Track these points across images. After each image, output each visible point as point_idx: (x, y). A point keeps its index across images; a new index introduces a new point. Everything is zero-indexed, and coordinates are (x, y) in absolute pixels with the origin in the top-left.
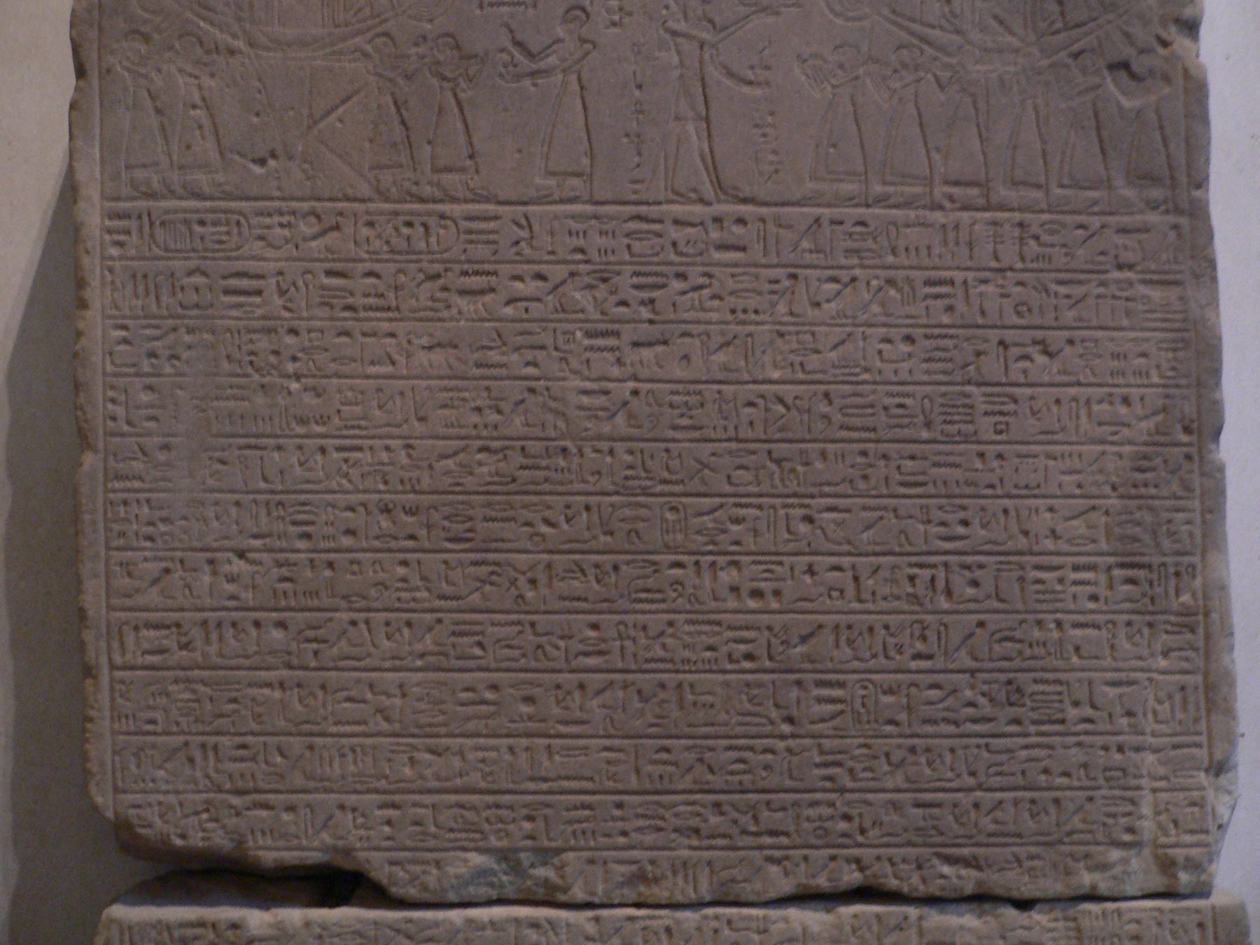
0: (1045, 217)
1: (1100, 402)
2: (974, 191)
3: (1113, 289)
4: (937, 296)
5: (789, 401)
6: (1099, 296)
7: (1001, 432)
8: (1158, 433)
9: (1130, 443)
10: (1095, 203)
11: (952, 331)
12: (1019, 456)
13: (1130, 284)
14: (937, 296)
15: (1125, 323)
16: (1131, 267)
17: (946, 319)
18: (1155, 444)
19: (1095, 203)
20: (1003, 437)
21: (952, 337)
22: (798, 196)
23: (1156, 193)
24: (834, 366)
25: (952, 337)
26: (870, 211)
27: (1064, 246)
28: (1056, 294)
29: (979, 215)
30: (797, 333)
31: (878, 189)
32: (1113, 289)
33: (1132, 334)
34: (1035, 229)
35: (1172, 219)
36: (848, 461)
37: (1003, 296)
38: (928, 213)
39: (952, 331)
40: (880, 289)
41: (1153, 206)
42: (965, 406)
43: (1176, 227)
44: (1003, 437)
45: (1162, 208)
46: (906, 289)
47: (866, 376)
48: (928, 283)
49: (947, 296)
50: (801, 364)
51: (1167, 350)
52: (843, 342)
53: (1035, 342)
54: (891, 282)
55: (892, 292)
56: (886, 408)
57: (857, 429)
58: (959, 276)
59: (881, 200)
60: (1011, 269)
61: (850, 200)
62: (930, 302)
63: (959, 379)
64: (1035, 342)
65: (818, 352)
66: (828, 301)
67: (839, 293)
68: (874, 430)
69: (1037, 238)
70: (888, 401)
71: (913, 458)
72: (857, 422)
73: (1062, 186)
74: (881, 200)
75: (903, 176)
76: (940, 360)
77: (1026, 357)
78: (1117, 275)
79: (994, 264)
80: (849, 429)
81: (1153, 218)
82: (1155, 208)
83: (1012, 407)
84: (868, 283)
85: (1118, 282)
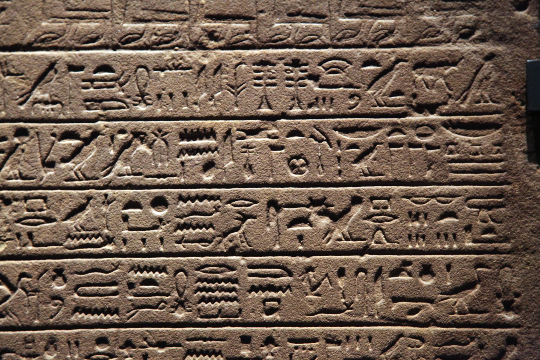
0: (329, 52)
1: (396, 273)
2: (243, 25)
3: (412, 135)
4: (193, 151)
5: (13, 280)
6: (392, 145)
7: (270, 311)
8: (471, 311)
9: (432, 321)
10: (391, 32)
11: (214, 191)
12: (291, 340)
13: (432, 126)
14: (193, 151)
15: (428, 175)
16: (432, 108)
17: (207, 178)
18: (468, 325)
19: (391, 32)
20: (276, 317)
21: (211, 198)
22: (29, 37)
23: (466, 17)
24: (69, 236)
25: (211, 198)
26: (118, 52)
27: (350, 86)
28: (339, 142)
29: (248, 53)
30: (26, 198)
31: (129, 26)
32: (412, 135)
33: (438, 189)
34: (314, 68)
35: (488, 48)
36: (84, 349)
37: (274, 148)
38: (183, 52)
39: (214, 191)
40: (127, 145)
41: (466, 33)
42: (226, 280)
43: (490, 57)
44: (276, 317)
45: (478, 33)
46: (159, 142)
47: (109, 247)
48: (185, 135)
49: (207, 149)
50: (30, 235)
51: (481, 207)
52: (82, 208)
53: (314, 202)
54: (137, 134)
55: (143, 148)
56: (131, 285)
57: (97, 311)
58: (221, 125)
59: (126, 41)
60: (284, 116)
61: (90, 41)
62: (187, 157)
63: (222, 247)
64: (314, 202)
65: (49, 220)
66: (64, 160)
67: (77, 151)
68: (116, 311)
69: (315, 77)
70: (134, 276)
71: (161, 344)
72: (98, 302)
73: (349, 15)
74: (126, 41)
75: (157, 11)
76: (198, 226)
77: (304, 220)
78: (417, 118)
79: (265, 110)
80: (87, 311)
81: (465, 47)
82: (465, 36)
83: (286, 279)
84: (112, 137)
85: (416, 126)
